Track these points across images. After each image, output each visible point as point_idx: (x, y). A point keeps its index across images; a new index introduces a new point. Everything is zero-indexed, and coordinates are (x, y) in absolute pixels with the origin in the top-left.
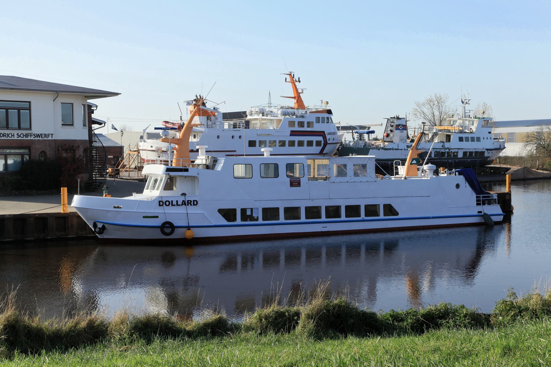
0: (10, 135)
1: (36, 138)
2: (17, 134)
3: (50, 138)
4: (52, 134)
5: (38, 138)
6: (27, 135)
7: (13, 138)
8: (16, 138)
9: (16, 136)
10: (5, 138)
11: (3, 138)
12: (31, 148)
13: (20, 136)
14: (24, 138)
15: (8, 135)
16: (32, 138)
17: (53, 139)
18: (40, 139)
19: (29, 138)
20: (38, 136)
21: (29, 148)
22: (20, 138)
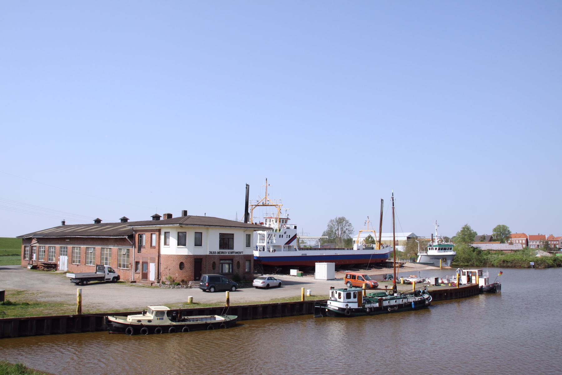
0: (225, 253)
1: (236, 254)
2: (228, 252)
3: (242, 254)
4: (243, 252)
5: (237, 254)
6: (232, 253)
7: (226, 254)
8: (227, 254)
9: (227, 253)
10: (223, 254)
11: (222, 254)
12: (234, 260)
13: (229, 253)
14: (231, 254)
15: (224, 253)
16: (234, 254)
17: (243, 254)
18: (238, 254)
19: (233, 254)
20: (237, 253)
21: (232, 260)
22: (229, 254)
